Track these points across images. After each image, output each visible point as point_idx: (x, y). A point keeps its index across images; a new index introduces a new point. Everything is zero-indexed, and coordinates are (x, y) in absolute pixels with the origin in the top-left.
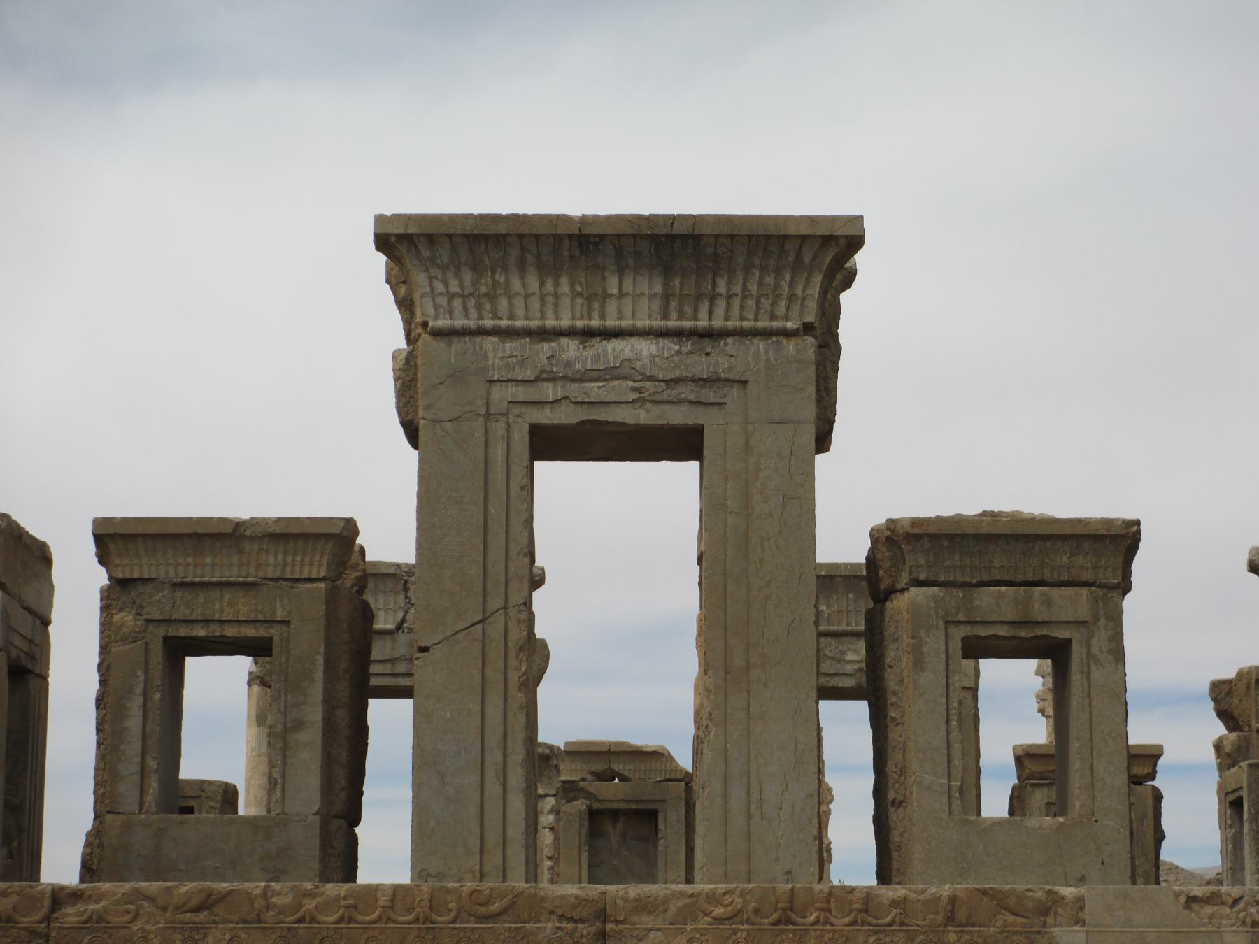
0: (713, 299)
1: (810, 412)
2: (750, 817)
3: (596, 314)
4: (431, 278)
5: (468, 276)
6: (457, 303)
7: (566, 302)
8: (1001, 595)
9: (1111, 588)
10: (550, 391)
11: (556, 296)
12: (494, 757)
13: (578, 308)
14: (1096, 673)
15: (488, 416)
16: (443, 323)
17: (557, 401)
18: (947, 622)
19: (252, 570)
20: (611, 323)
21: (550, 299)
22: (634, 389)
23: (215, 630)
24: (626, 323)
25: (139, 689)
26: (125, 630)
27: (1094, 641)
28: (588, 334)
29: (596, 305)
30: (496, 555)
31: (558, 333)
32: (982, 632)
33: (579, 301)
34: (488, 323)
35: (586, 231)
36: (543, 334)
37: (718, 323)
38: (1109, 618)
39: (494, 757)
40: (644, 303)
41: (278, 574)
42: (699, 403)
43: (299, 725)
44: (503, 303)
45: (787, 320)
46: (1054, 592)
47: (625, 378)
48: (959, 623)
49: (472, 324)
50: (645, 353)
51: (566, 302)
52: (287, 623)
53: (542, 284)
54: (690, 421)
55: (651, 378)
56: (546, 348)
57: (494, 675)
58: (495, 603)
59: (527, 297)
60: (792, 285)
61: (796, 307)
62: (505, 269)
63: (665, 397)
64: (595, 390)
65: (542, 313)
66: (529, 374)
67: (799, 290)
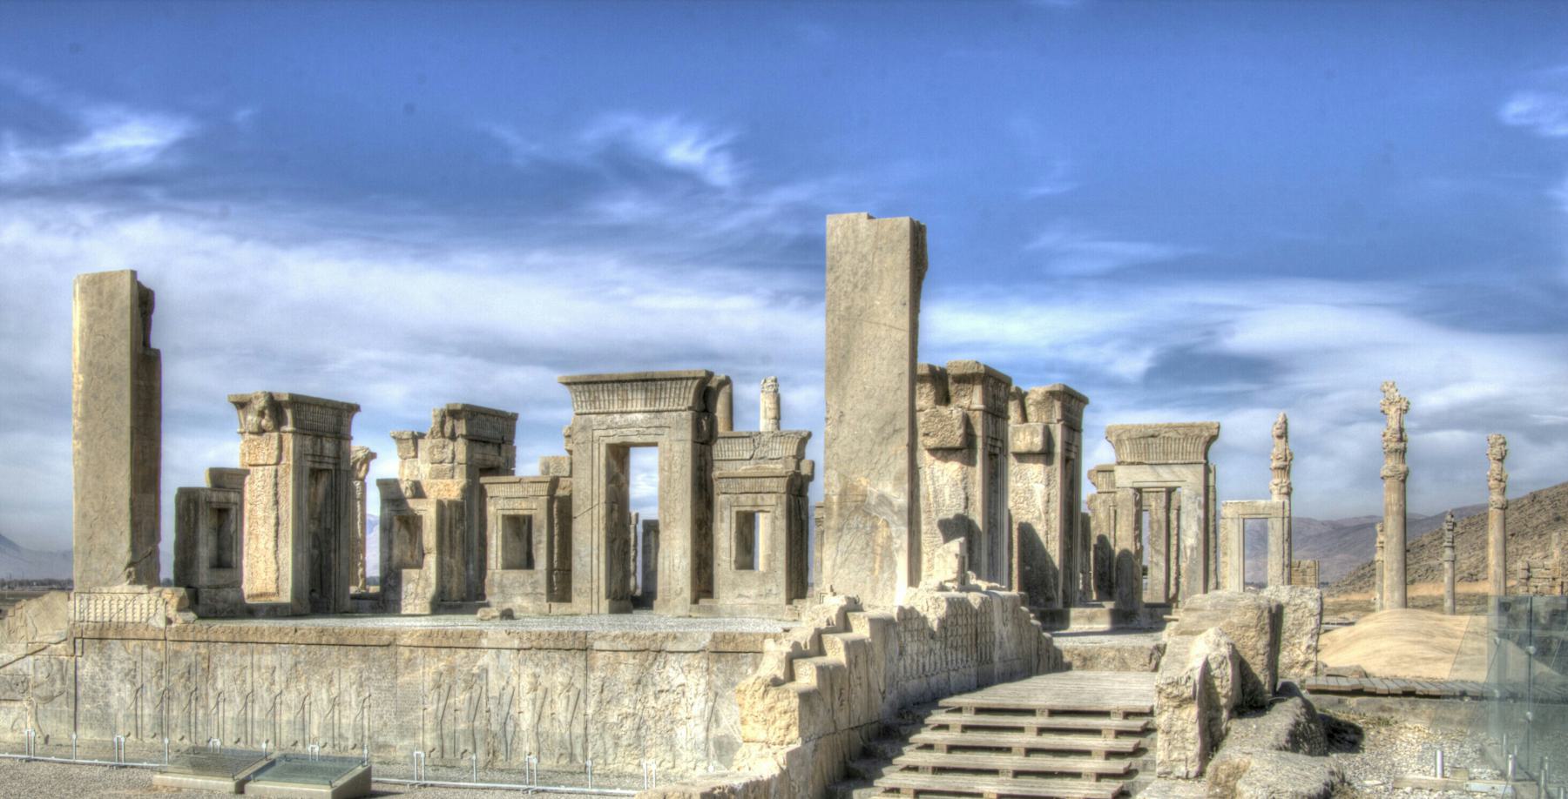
0: (660, 399)
5: (587, 394)
10: (611, 432)
12: (595, 552)
24: (633, 409)
28: (622, 413)
31: (613, 413)
34: (592, 411)
37: (662, 408)
39: (595, 552)
43: (540, 542)
46: (765, 496)
51: (616, 402)
58: (595, 502)
62: (598, 391)
66: (605, 427)
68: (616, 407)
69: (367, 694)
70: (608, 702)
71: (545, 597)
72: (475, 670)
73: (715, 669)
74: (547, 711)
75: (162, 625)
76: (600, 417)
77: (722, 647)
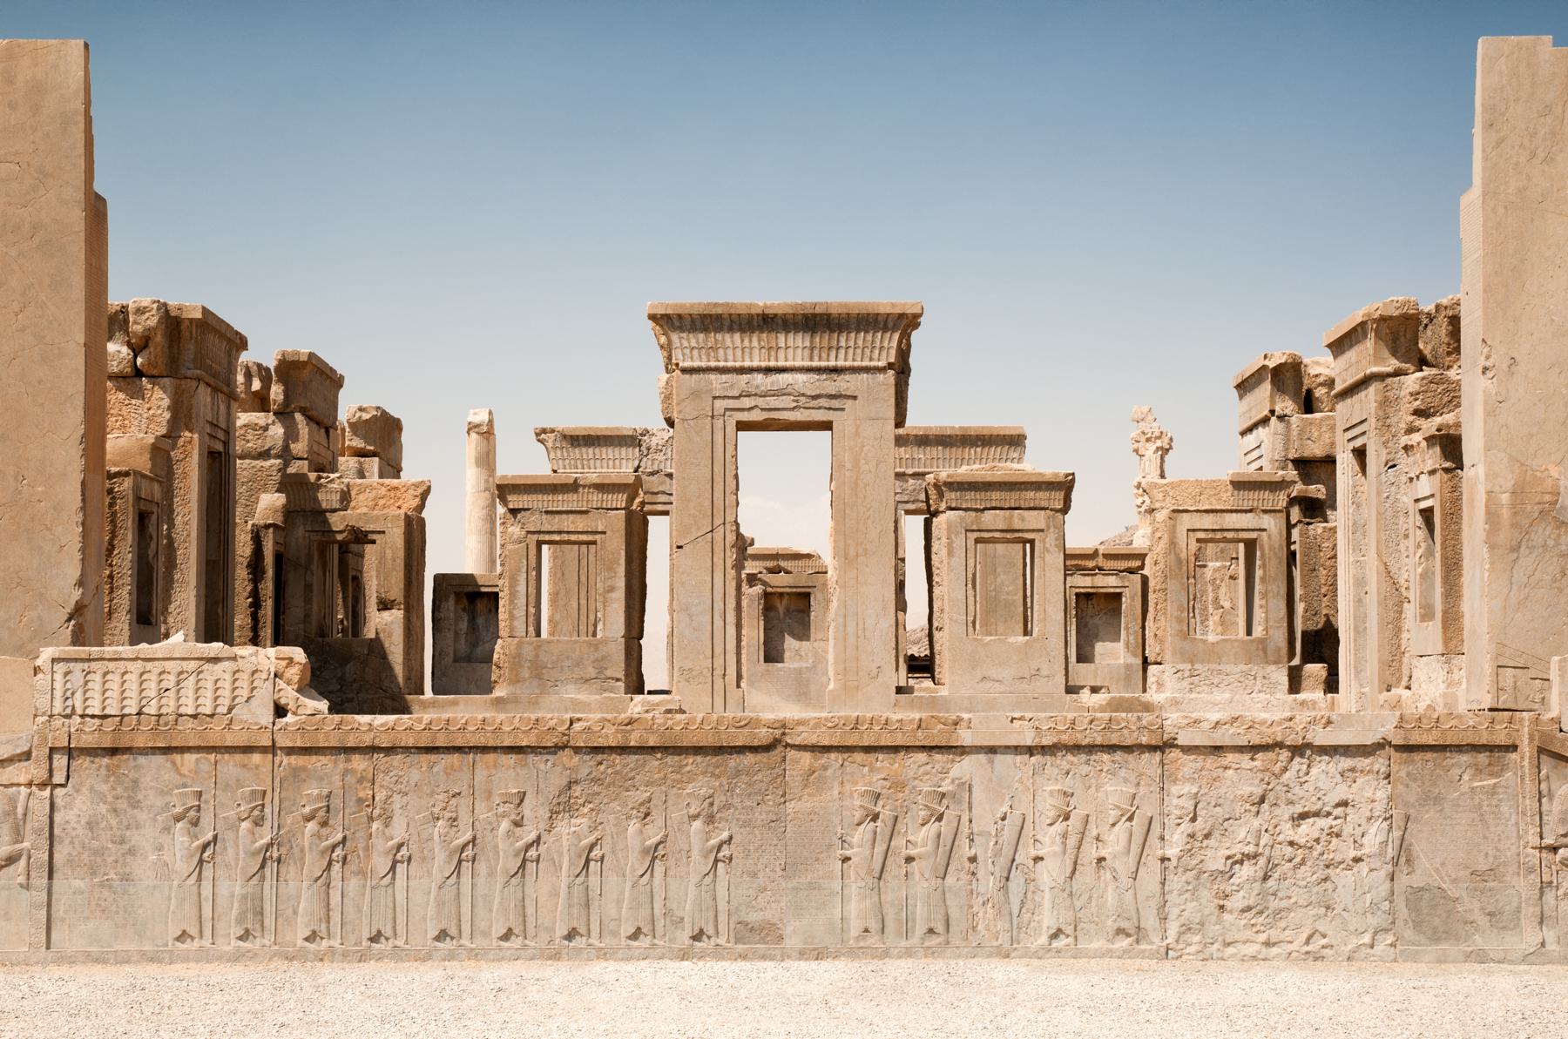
1: (891, 413)
2: (858, 637)
3: (772, 358)
4: (680, 338)
6: (695, 352)
7: (756, 351)
8: (996, 515)
9: (1057, 511)
10: (747, 402)
11: (751, 348)
12: (719, 606)
13: (762, 355)
14: (1048, 558)
15: (713, 417)
16: (687, 364)
17: (752, 408)
18: (967, 531)
19: (585, 503)
20: (781, 363)
21: (747, 350)
22: (794, 401)
23: (565, 537)
24: (789, 364)
25: (524, 569)
26: (515, 537)
27: (1048, 540)
28: (768, 371)
29: (773, 353)
30: (718, 495)
31: (751, 370)
32: (986, 535)
33: (763, 350)
34: (713, 364)
35: (767, 312)
36: (742, 371)
37: (841, 363)
38: (1055, 527)
39: (719, 606)
40: (799, 351)
41: (599, 505)
42: (830, 409)
43: (612, 589)
44: (721, 352)
45: (879, 360)
47: (789, 395)
48: (973, 531)
49: (703, 364)
50: (800, 380)
51: (756, 351)
52: (604, 533)
53: (742, 341)
54: (825, 419)
55: (803, 395)
57: (718, 560)
58: (718, 521)
59: (734, 348)
60: (881, 341)
61: (884, 353)
63: (811, 405)
64: (773, 402)
65: (743, 358)
67: (886, 344)
68: (756, 358)
69: (725, 835)
70: (1207, 836)
71: (621, 685)
72: (946, 787)
73: (1403, 774)
74: (1091, 852)
75: (266, 716)
77: (1416, 738)
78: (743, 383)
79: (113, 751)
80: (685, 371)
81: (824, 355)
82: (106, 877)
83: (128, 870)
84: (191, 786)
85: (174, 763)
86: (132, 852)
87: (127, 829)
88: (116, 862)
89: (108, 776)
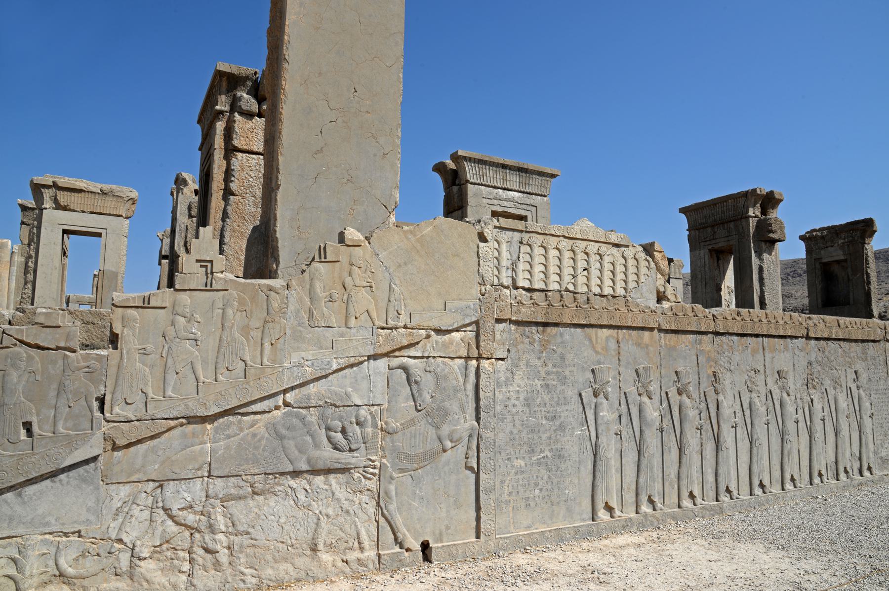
6: (475, 176)
10: (496, 202)
22: (515, 205)
36: (495, 187)
44: (485, 178)
56: (495, 191)
64: (505, 203)
66: (491, 197)
75: (652, 303)
76: (488, 189)
78: (495, 193)
79: (545, 325)
80: (472, 183)
81: (524, 186)
82: (542, 455)
83: (559, 446)
84: (604, 363)
85: (590, 340)
86: (562, 428)
87: (558, 405)
88: (550, 438)
89: (541, 352)
